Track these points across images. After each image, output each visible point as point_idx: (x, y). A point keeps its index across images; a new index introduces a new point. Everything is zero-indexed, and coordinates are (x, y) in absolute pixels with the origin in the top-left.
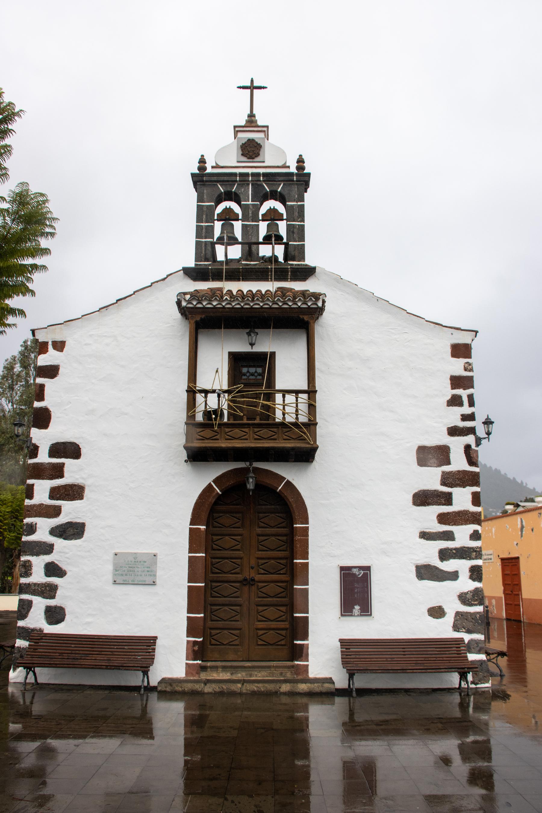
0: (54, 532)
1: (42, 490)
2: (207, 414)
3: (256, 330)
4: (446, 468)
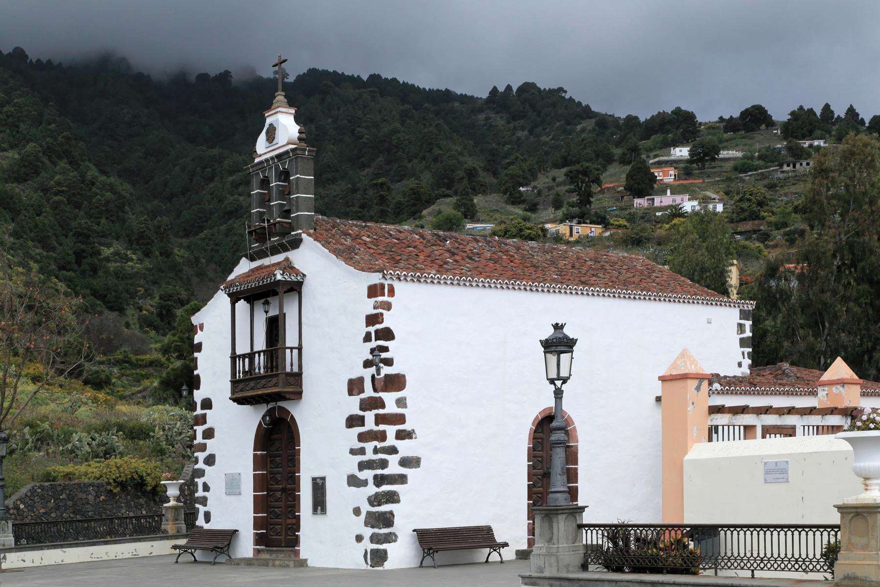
4: (363, 396)
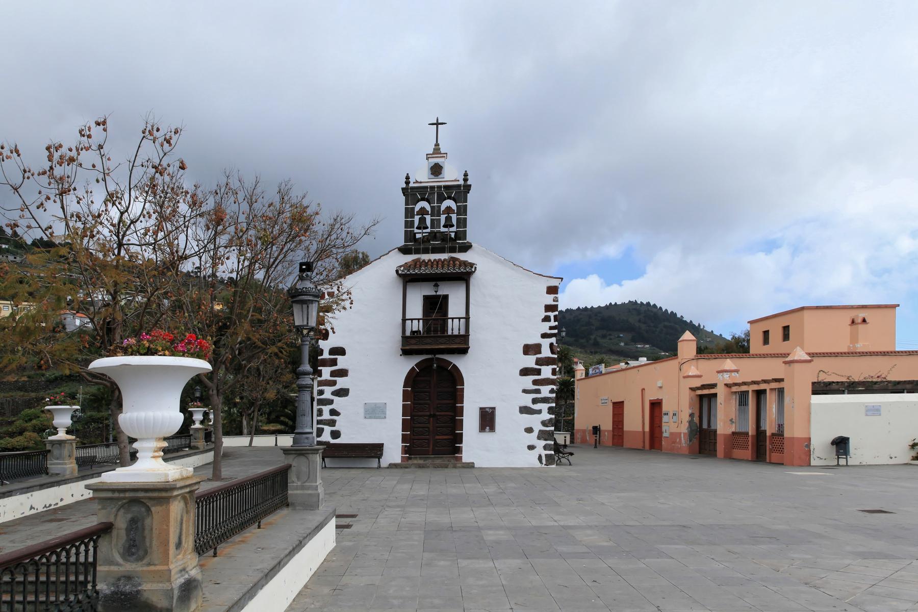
0: (334, 393)
1: (326, 372)
2: (413, 332)
3: (439, 283)
4: (539, 356)
